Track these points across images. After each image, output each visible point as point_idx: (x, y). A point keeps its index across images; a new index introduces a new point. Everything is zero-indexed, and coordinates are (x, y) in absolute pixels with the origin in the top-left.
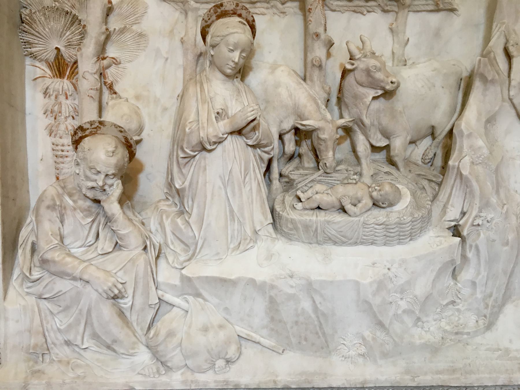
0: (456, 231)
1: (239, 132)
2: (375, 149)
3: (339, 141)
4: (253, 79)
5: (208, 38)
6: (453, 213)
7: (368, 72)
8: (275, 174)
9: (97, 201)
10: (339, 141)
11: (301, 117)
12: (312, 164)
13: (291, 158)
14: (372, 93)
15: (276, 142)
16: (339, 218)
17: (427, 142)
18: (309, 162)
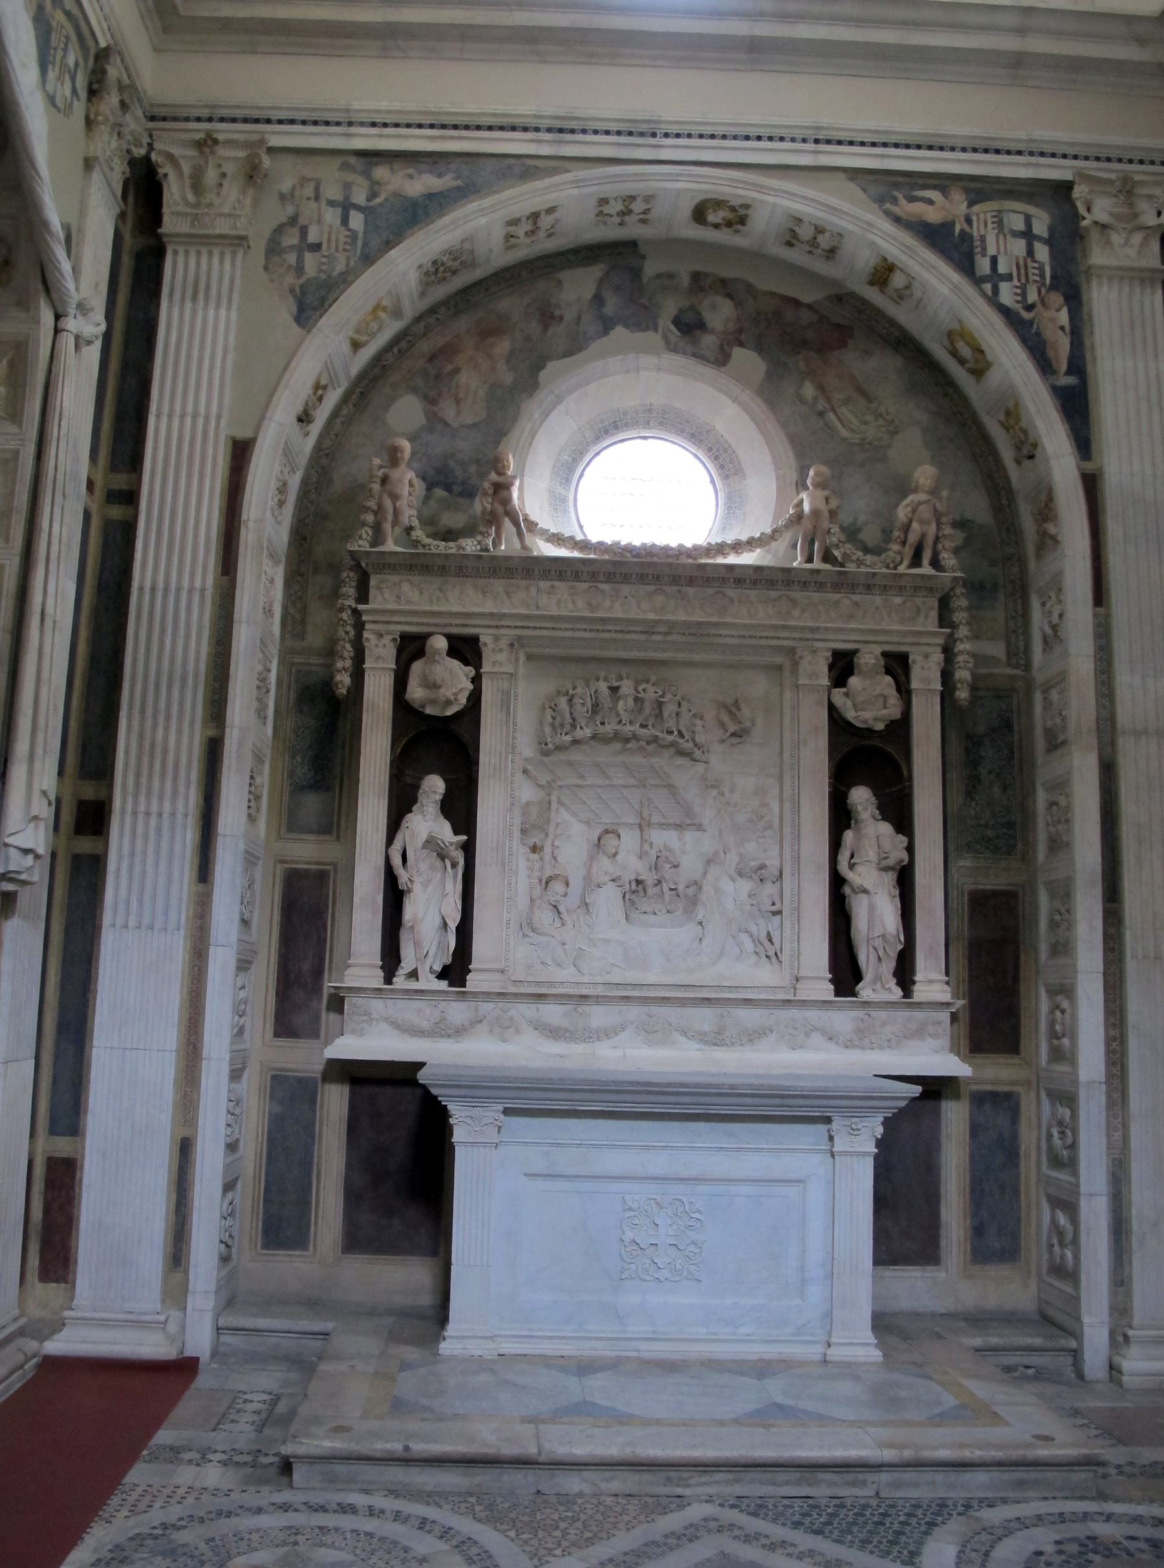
0: (700, 923)
1: (613, 880)
2: (671, 890)
3: (656, 885)
4: (618, 857)
5: (601, 841)
6: (700, 917)
7: (667, 857)
8: (627, 897)
9: (555, 907)
10: (656, 885)
11: (638, 874)
12: (643, 895)
13: (634, 892)
14: (669, 866)
15: (628, 885)
16: (653, 917)
17: (695, 887)
18: (641, 894)
